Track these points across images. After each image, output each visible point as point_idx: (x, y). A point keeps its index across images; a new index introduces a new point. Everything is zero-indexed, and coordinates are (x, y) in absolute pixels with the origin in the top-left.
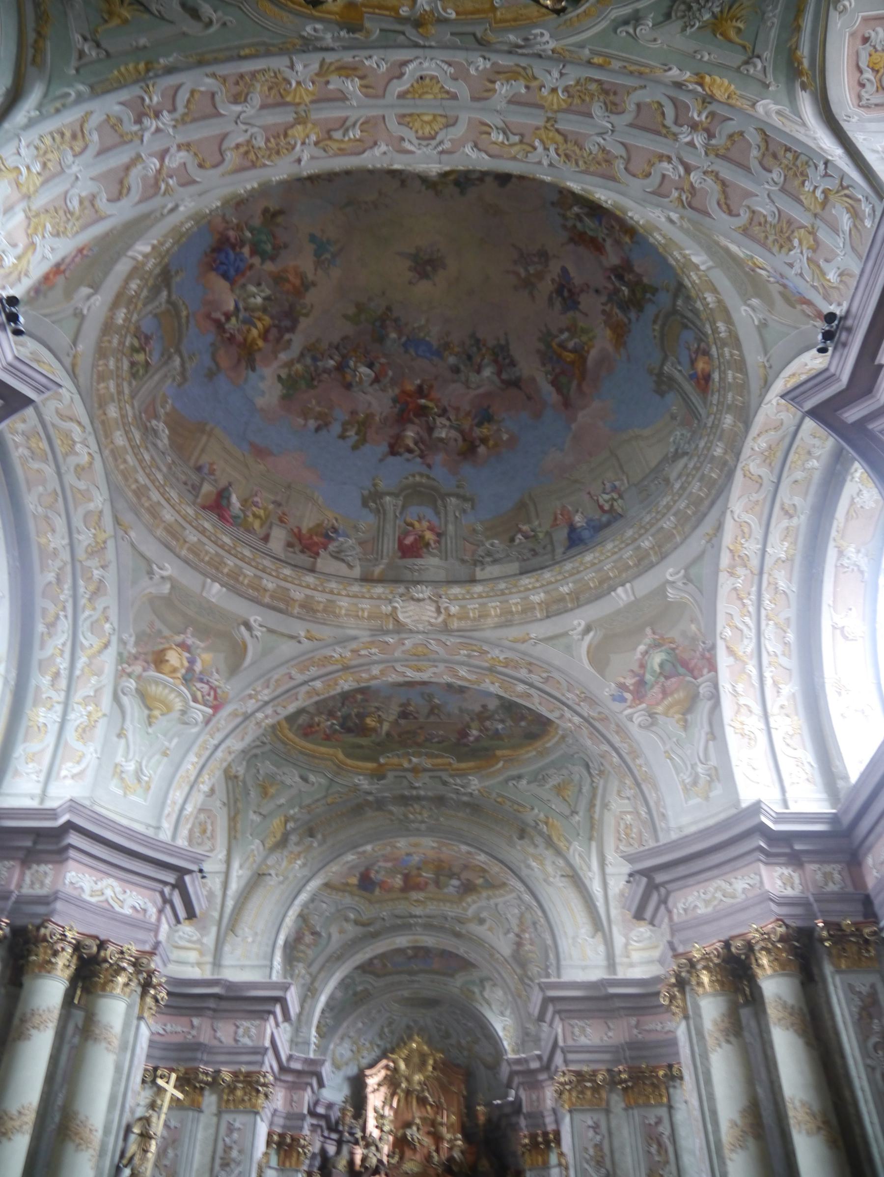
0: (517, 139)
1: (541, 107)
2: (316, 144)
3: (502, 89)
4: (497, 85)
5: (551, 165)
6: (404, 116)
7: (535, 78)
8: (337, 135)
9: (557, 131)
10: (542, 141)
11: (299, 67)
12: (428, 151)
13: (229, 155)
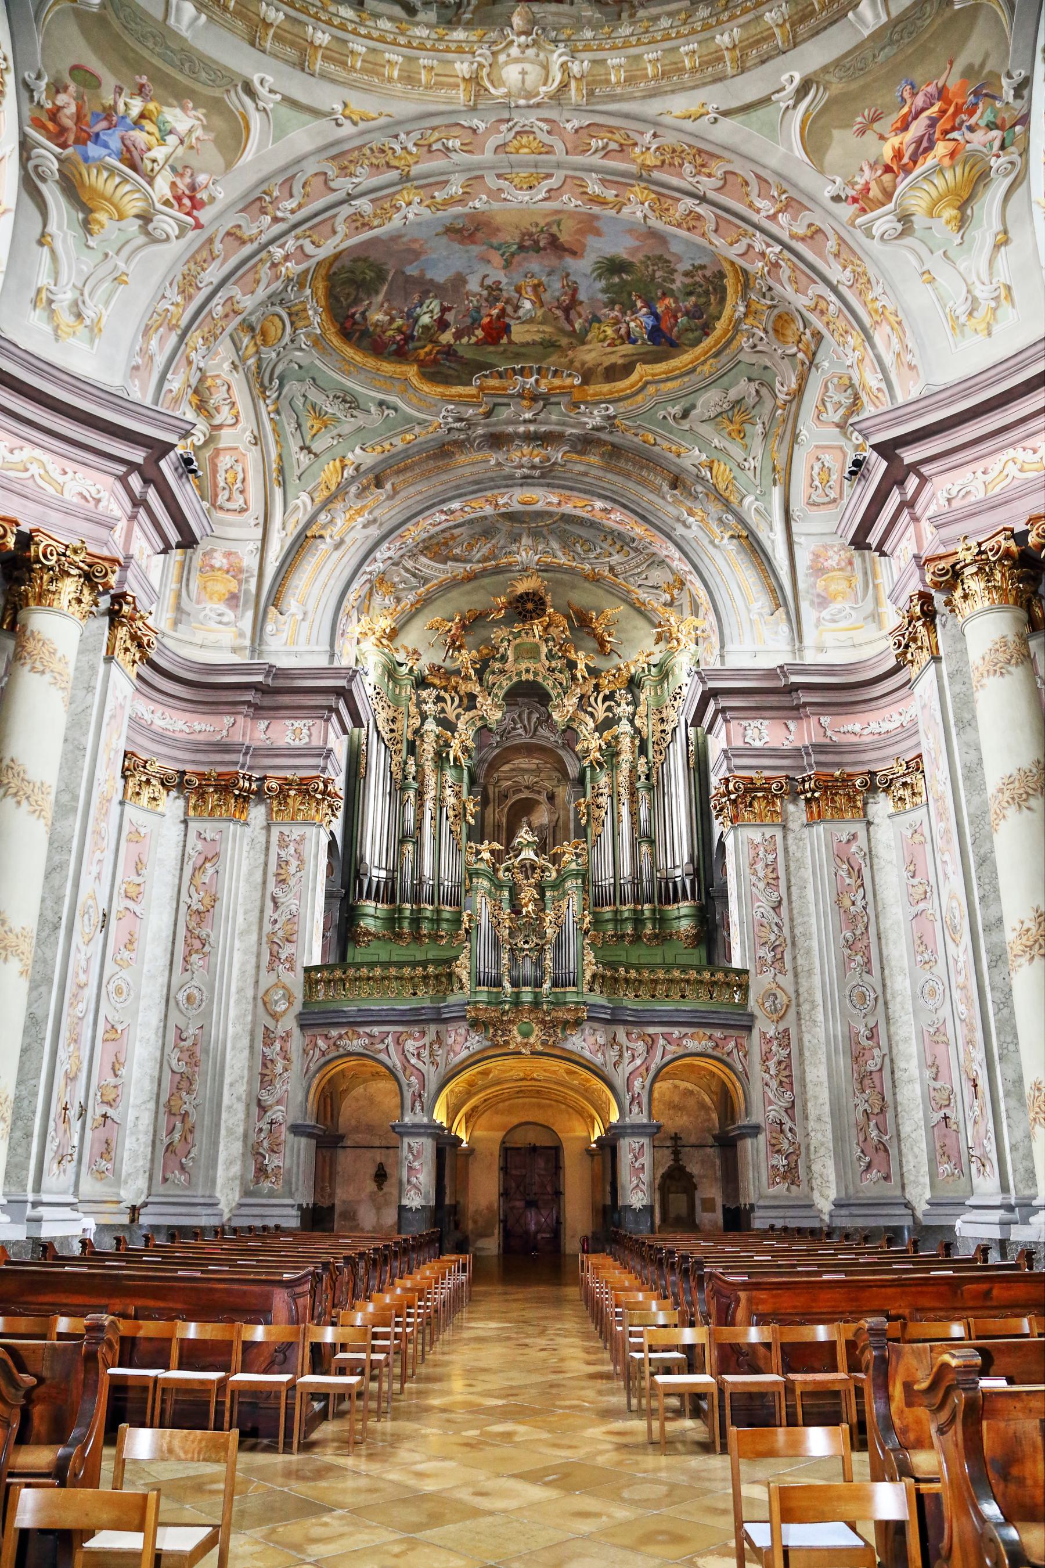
0: (434, 147)
1: (416, 188)
2: (636, 144)
3: (455, 189)
4: (460, 191)
5: (396, 136)
6: (547, 153)
7: (428, 206)
8: (613, 146)
9: (397, 168)
10: (410, 153)
11: (639, 214)
12: (523, 121)
13: (719, 173)
